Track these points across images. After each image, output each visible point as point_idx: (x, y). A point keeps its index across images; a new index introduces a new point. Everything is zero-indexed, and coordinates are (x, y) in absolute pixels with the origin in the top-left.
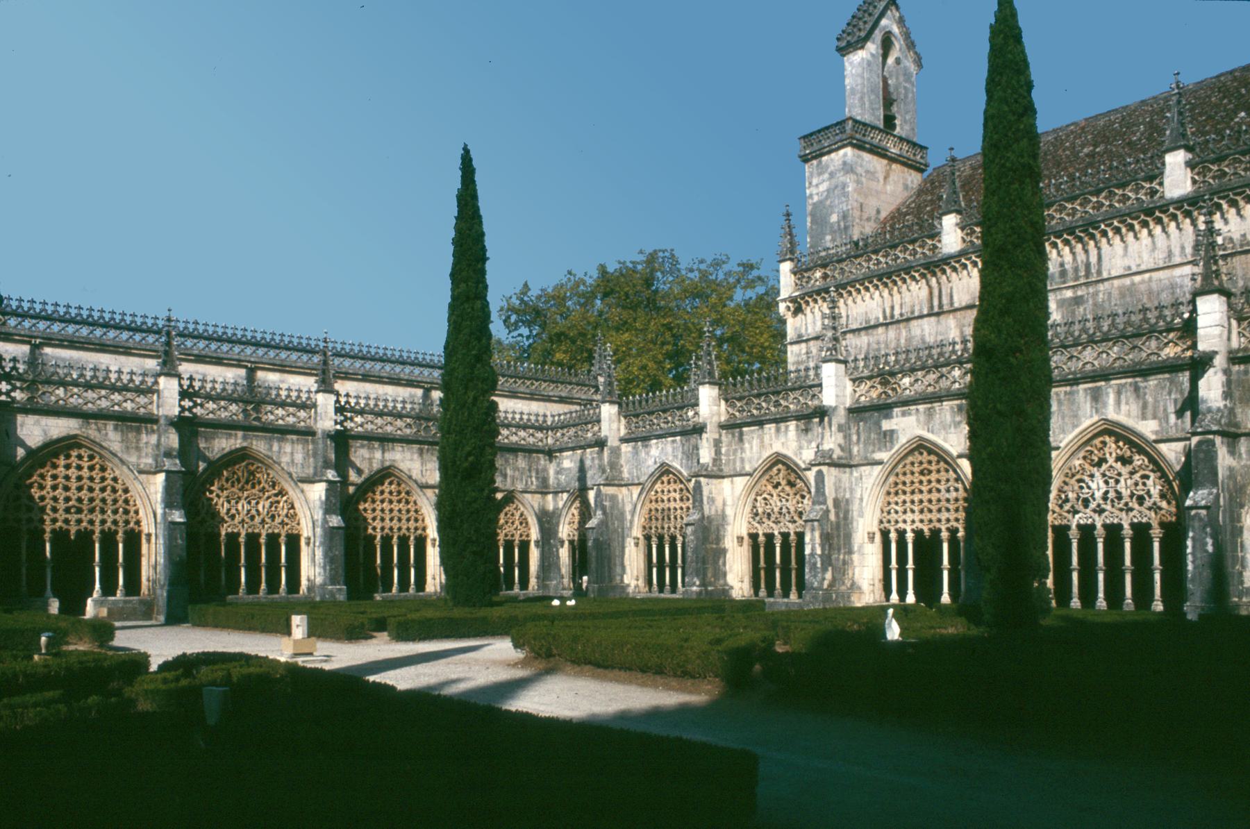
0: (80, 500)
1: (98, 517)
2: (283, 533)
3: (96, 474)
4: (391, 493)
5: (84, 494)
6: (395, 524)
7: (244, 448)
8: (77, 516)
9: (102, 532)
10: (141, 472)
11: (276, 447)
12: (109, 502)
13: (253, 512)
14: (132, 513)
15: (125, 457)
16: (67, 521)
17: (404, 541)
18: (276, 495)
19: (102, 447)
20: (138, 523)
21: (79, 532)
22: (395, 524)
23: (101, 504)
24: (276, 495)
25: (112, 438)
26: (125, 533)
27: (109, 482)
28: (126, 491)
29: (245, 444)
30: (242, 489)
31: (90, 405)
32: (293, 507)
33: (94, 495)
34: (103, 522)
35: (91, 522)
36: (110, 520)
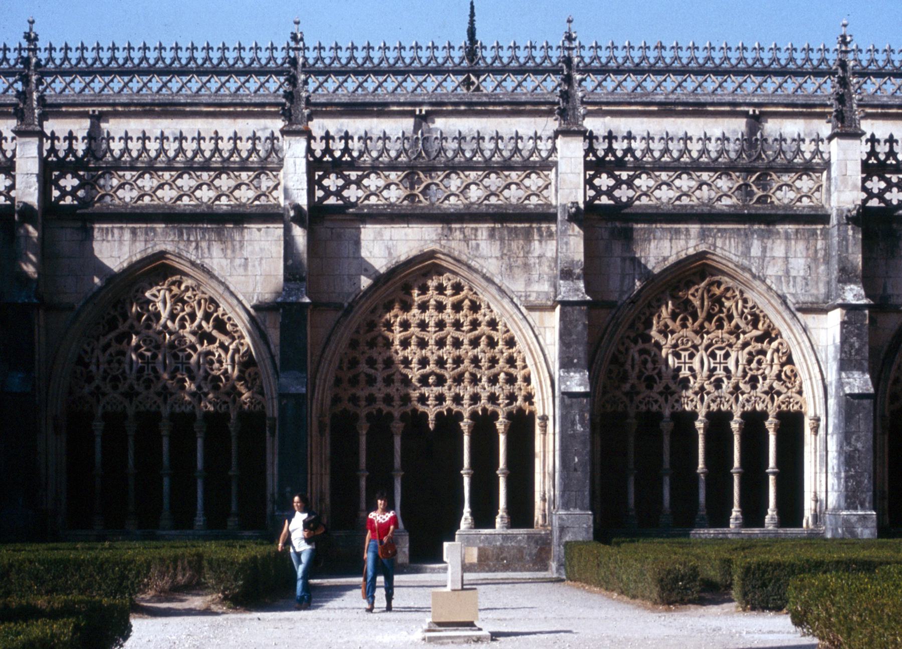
0: (441, 362)
1: (466, 391)
2: (772, 412)
3: (465, 316)
5: (448, 352)
7: (702, 255)
8: (437, 390)
9: (474, 415)
10: (531, 308)
11: (756, 249)
12: (484, 363)
13: (720, 373)
14: (520, 382)
15: (507, 284)
18: (760, 339)
19: (469, 267)
20: (529, 398)
21: (439, 415)
23: (471, 368)
24: (760, 339)
25: (484, 249)
26: (509, 416)
27: (483, 328)
28: (511, 343)
29: (702, 248)
30: (700, 331)
32: (790, 361)
33: (461, 352)
34: (475, 398)
35: (458, 399)
36: (484, 395)
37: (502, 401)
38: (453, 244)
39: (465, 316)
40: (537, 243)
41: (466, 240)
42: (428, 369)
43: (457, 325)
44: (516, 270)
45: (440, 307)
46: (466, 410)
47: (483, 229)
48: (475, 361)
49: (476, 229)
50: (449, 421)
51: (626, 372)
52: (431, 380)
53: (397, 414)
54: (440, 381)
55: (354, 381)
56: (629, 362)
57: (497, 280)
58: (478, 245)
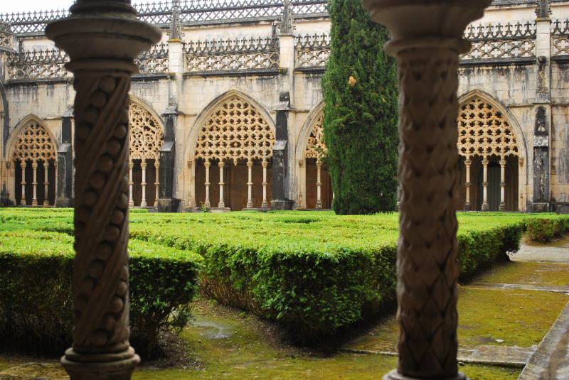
1: (250, 149)
4: (481, 116)
5: (242, 133)
6: (485, 145)
9: (253, 160)
12: (257, 138)
16: (232, 153)
17: (494, 162)
21: (238, 160)
22: (485, 145)
27: (257, 123)
31: (243, 67)
36: (257, 151)
37: (264, 153)
38: (241, 86)
39: (249, 117)
40: (276, 85)
41: (246, 84)
42: (233, 141)
43: (246, 121)
44: (267, 97)
45: (239, 114)
46: (249, 158)
47: (254, 78)
48: (253, 136)
49: (251, 80)
50: (243, 162)
51: (316, 140)
52: (236, 144)
53: (221, 159)
54: (239, 145)
55: (204, 145)
56: (318, 136)
57: (260, 102)
58: (252, 87)
